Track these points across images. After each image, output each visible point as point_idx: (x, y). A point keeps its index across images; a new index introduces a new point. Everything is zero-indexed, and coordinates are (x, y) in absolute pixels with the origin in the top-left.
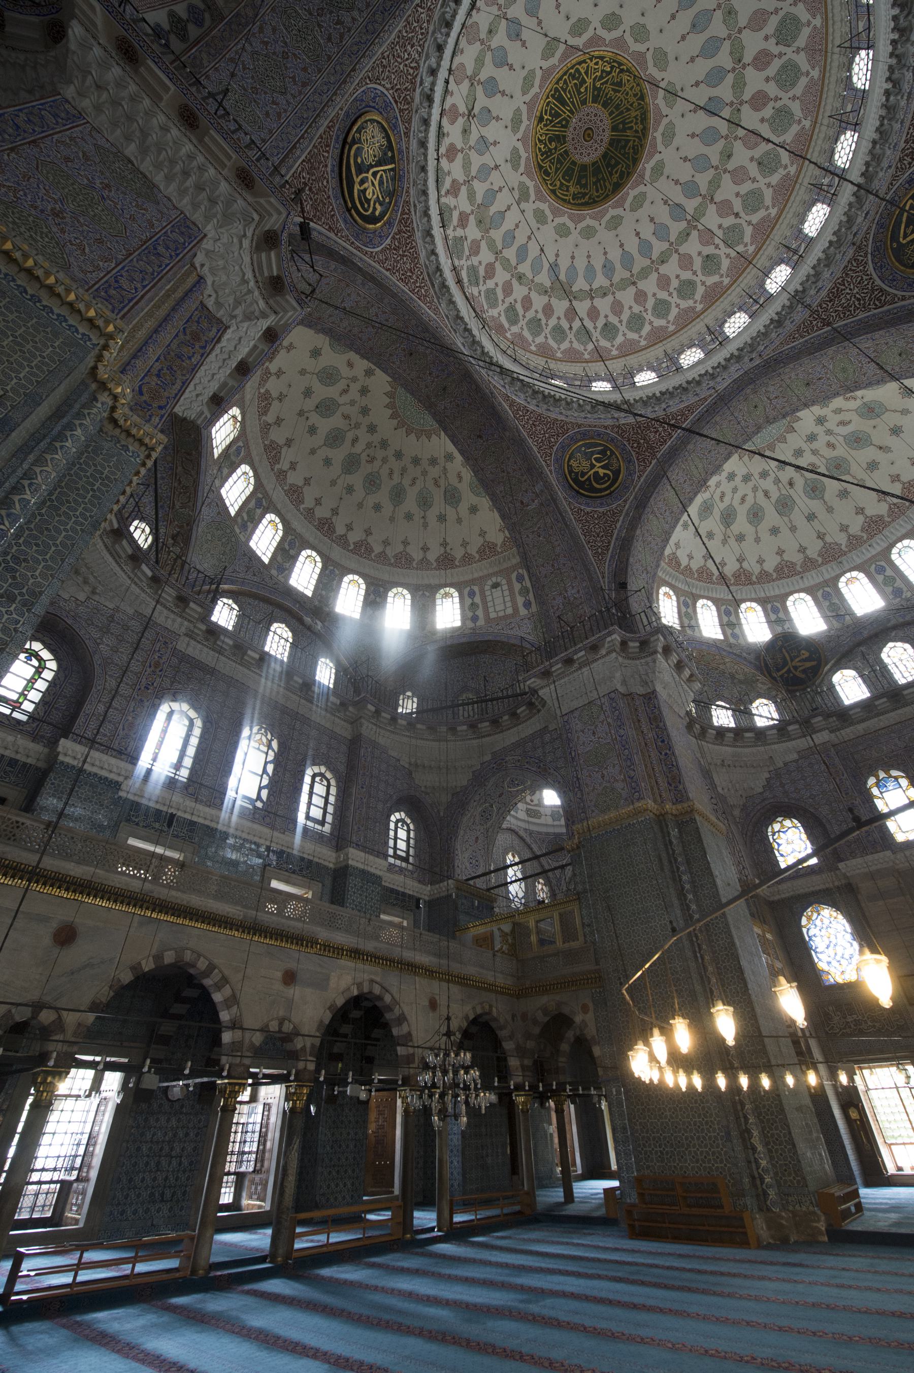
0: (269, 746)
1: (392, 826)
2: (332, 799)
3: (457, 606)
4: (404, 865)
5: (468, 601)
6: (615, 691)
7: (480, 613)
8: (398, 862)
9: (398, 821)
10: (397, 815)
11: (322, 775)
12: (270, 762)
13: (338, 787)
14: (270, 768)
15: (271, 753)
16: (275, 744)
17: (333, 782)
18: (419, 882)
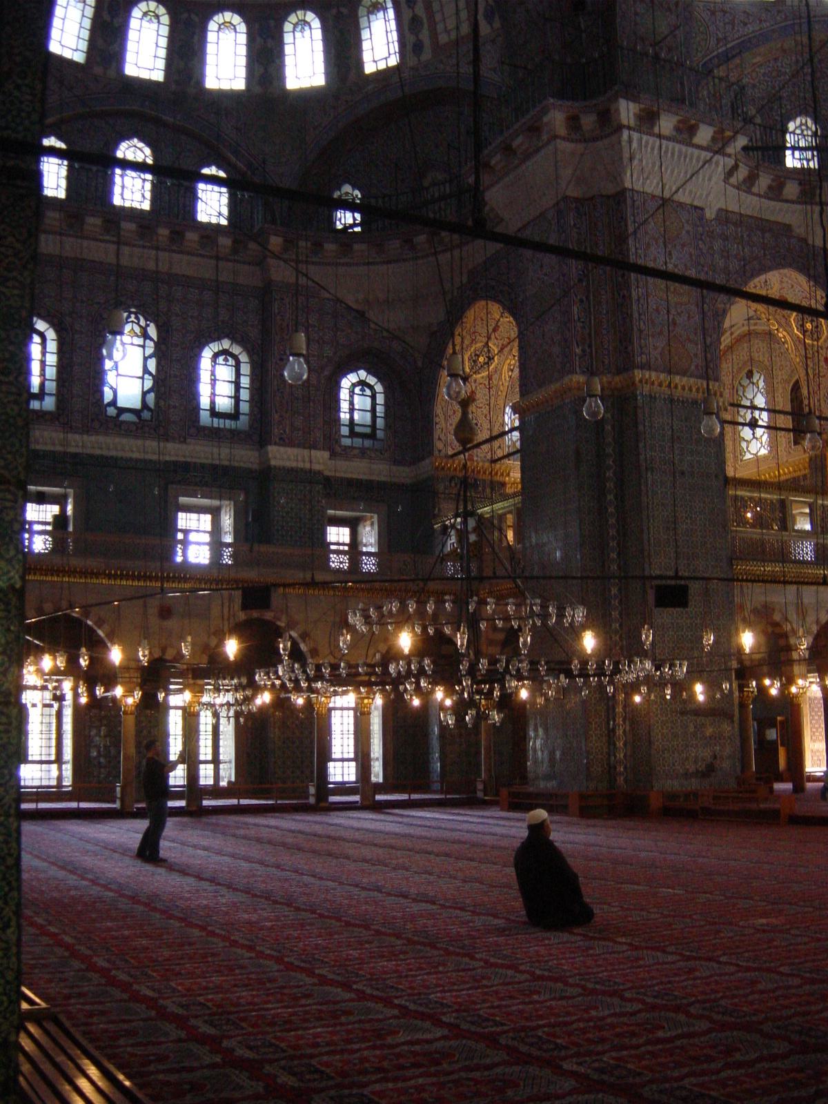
0: (145, 335)
1: (344, 394)
2: (245, 381)
3: (393, 25)
4: (368, 443)
5: (408, 14)
6: (566, 198)
7: (425, 35)
8: (358, 442)
9: (354, 385)
10: (352, 378)
11: (225, 352)
12: (150, 357)
13: (253, 364)
14: (152, 365)
15: (150, 344)
16: (152, 331)
17: (244, 358)
18: (397, 462)
